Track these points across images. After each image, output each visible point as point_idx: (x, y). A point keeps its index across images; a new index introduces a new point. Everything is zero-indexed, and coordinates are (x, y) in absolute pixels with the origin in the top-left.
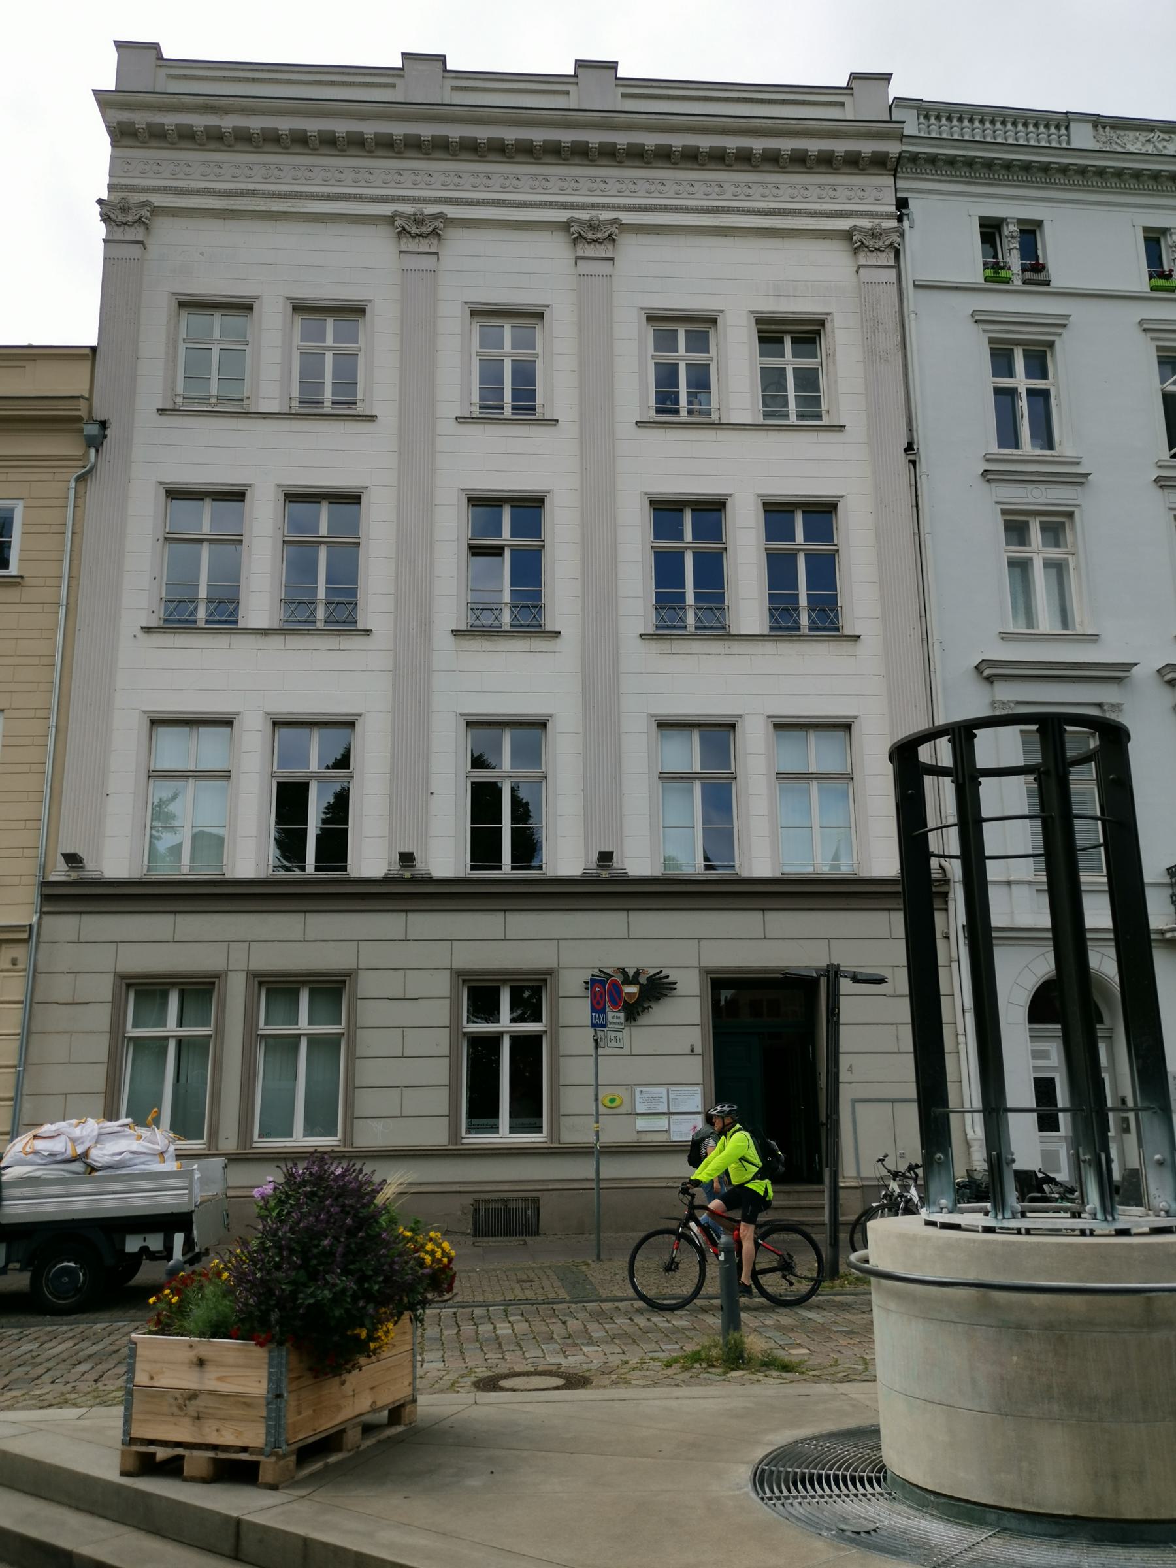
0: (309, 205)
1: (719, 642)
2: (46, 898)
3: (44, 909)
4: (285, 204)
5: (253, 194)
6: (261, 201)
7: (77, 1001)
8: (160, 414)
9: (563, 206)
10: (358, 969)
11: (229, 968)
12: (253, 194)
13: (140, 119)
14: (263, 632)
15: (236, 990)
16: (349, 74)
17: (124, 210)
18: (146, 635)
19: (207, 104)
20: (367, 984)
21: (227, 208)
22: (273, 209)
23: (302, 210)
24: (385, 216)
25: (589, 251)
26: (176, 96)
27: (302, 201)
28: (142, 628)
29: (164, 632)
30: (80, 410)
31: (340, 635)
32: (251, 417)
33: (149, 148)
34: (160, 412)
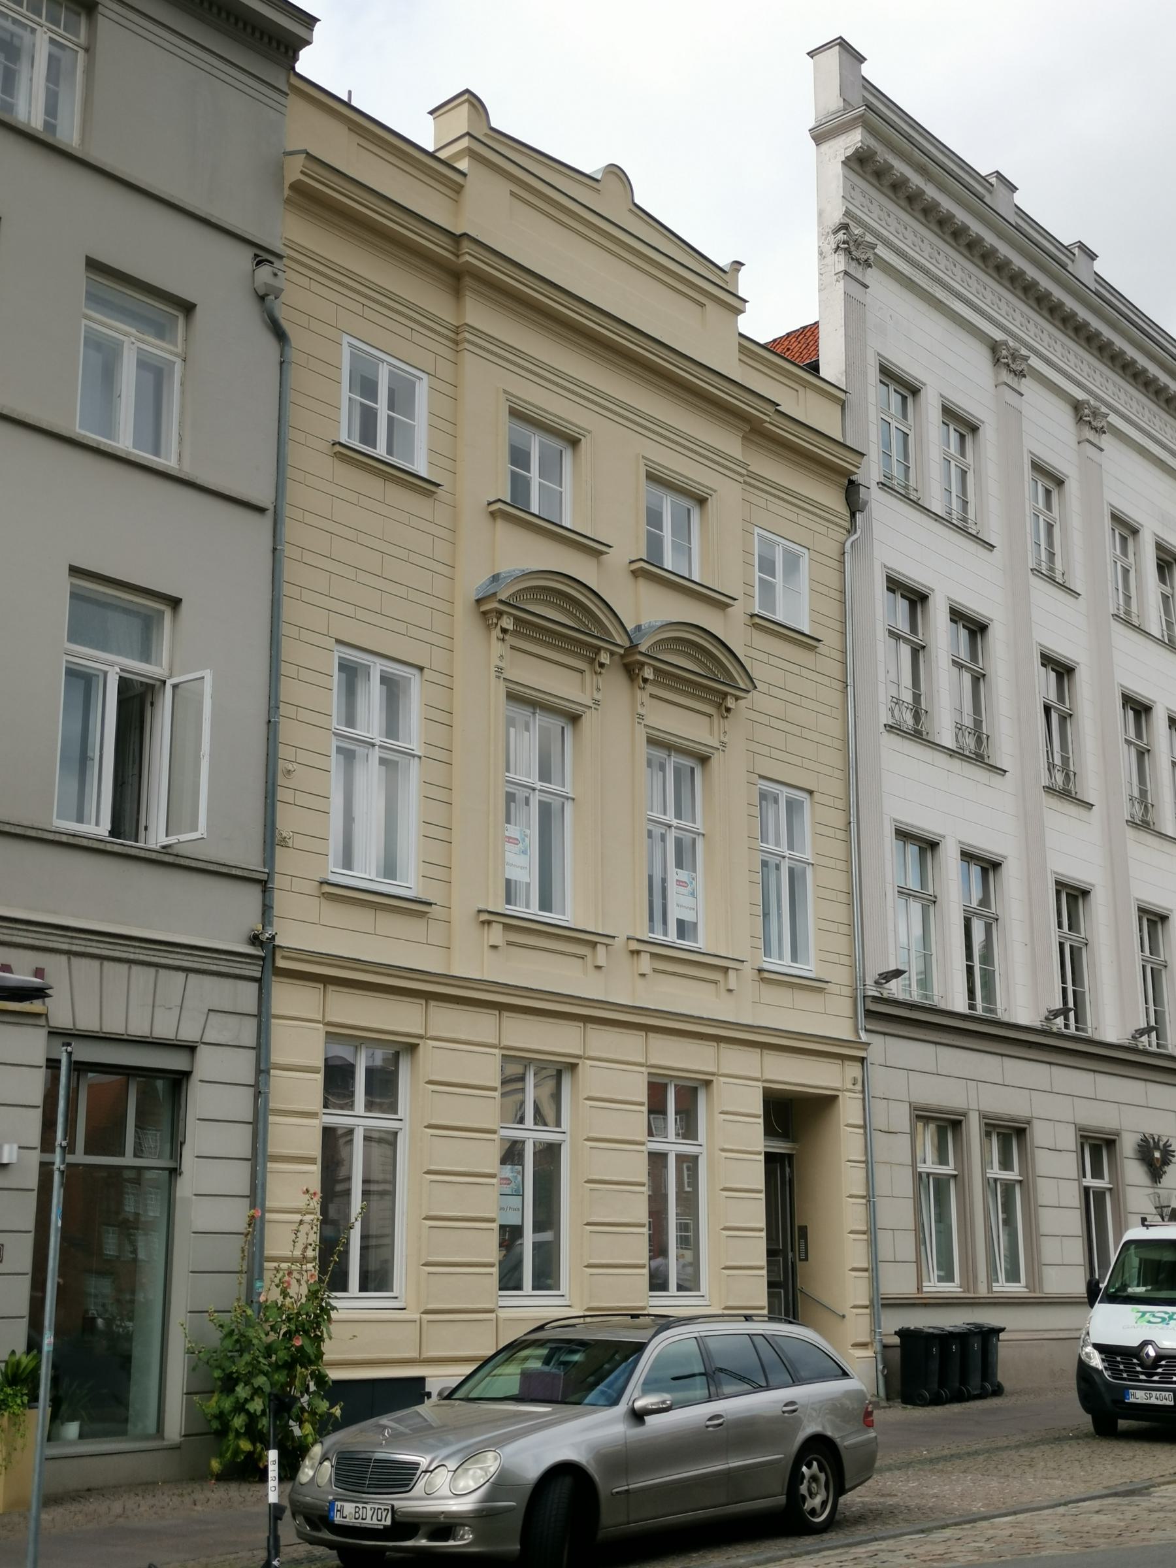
0: (955, 303)
1: (1158, 839)
2: (869, 1014)
3: (868, 1027)
4: (942, 293)
5: (926, 272)
6: (930, 282)
7: (890, 1131)
8: (880, 488)
9: (1079, 385)
10: (1032, 1117)
11: (971, 1108)
12: (926, 272)
13: (884, 155)
14: (952, 753)
15: (974, 1128)
16: (963, 169)
17: (858, 244)
18: (886, 733)
19: (925, 165)
20: (1040, 1134)
21: (912, 277)
22: (937, 295)
23: (952, 306)
24: (992, 338)
25: (1089, 434)
26: (912, 146)
27: (952, 296)
28: (885, 725)
29: (898, 734)
30: (858, 468)
31: (990, 770)
32: (929, 516)
33: (864, 179)
34: (881, 486)
